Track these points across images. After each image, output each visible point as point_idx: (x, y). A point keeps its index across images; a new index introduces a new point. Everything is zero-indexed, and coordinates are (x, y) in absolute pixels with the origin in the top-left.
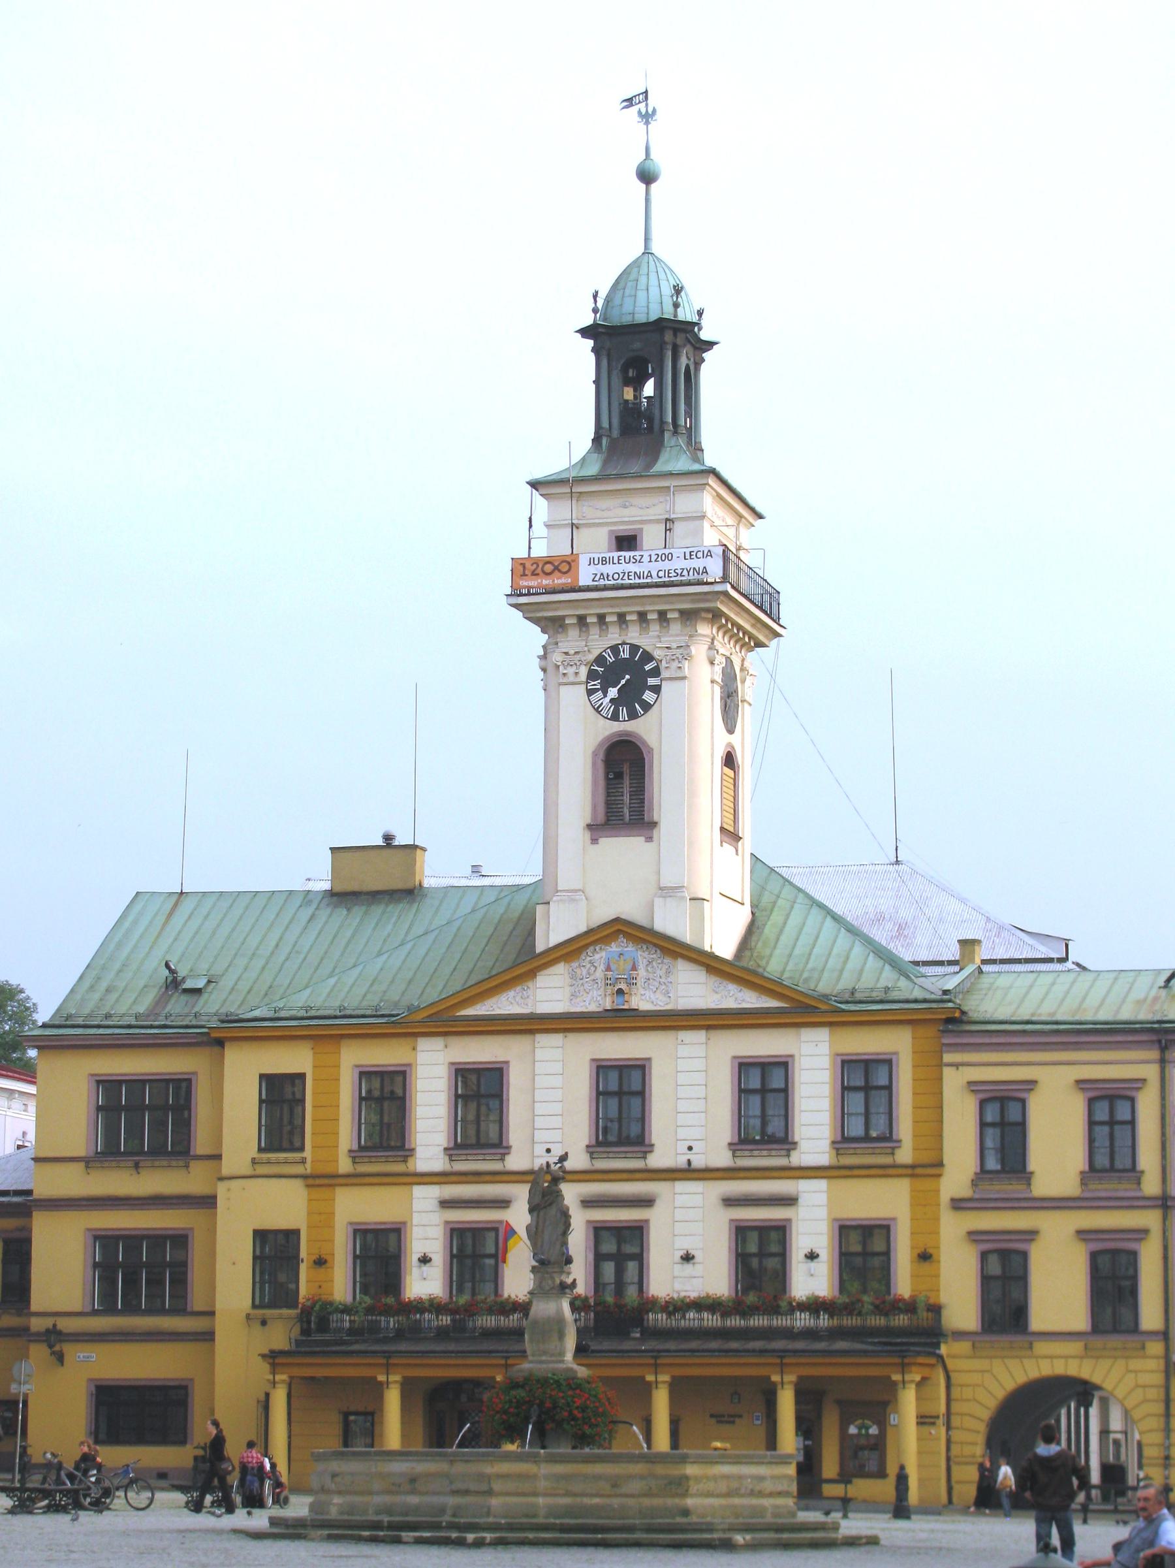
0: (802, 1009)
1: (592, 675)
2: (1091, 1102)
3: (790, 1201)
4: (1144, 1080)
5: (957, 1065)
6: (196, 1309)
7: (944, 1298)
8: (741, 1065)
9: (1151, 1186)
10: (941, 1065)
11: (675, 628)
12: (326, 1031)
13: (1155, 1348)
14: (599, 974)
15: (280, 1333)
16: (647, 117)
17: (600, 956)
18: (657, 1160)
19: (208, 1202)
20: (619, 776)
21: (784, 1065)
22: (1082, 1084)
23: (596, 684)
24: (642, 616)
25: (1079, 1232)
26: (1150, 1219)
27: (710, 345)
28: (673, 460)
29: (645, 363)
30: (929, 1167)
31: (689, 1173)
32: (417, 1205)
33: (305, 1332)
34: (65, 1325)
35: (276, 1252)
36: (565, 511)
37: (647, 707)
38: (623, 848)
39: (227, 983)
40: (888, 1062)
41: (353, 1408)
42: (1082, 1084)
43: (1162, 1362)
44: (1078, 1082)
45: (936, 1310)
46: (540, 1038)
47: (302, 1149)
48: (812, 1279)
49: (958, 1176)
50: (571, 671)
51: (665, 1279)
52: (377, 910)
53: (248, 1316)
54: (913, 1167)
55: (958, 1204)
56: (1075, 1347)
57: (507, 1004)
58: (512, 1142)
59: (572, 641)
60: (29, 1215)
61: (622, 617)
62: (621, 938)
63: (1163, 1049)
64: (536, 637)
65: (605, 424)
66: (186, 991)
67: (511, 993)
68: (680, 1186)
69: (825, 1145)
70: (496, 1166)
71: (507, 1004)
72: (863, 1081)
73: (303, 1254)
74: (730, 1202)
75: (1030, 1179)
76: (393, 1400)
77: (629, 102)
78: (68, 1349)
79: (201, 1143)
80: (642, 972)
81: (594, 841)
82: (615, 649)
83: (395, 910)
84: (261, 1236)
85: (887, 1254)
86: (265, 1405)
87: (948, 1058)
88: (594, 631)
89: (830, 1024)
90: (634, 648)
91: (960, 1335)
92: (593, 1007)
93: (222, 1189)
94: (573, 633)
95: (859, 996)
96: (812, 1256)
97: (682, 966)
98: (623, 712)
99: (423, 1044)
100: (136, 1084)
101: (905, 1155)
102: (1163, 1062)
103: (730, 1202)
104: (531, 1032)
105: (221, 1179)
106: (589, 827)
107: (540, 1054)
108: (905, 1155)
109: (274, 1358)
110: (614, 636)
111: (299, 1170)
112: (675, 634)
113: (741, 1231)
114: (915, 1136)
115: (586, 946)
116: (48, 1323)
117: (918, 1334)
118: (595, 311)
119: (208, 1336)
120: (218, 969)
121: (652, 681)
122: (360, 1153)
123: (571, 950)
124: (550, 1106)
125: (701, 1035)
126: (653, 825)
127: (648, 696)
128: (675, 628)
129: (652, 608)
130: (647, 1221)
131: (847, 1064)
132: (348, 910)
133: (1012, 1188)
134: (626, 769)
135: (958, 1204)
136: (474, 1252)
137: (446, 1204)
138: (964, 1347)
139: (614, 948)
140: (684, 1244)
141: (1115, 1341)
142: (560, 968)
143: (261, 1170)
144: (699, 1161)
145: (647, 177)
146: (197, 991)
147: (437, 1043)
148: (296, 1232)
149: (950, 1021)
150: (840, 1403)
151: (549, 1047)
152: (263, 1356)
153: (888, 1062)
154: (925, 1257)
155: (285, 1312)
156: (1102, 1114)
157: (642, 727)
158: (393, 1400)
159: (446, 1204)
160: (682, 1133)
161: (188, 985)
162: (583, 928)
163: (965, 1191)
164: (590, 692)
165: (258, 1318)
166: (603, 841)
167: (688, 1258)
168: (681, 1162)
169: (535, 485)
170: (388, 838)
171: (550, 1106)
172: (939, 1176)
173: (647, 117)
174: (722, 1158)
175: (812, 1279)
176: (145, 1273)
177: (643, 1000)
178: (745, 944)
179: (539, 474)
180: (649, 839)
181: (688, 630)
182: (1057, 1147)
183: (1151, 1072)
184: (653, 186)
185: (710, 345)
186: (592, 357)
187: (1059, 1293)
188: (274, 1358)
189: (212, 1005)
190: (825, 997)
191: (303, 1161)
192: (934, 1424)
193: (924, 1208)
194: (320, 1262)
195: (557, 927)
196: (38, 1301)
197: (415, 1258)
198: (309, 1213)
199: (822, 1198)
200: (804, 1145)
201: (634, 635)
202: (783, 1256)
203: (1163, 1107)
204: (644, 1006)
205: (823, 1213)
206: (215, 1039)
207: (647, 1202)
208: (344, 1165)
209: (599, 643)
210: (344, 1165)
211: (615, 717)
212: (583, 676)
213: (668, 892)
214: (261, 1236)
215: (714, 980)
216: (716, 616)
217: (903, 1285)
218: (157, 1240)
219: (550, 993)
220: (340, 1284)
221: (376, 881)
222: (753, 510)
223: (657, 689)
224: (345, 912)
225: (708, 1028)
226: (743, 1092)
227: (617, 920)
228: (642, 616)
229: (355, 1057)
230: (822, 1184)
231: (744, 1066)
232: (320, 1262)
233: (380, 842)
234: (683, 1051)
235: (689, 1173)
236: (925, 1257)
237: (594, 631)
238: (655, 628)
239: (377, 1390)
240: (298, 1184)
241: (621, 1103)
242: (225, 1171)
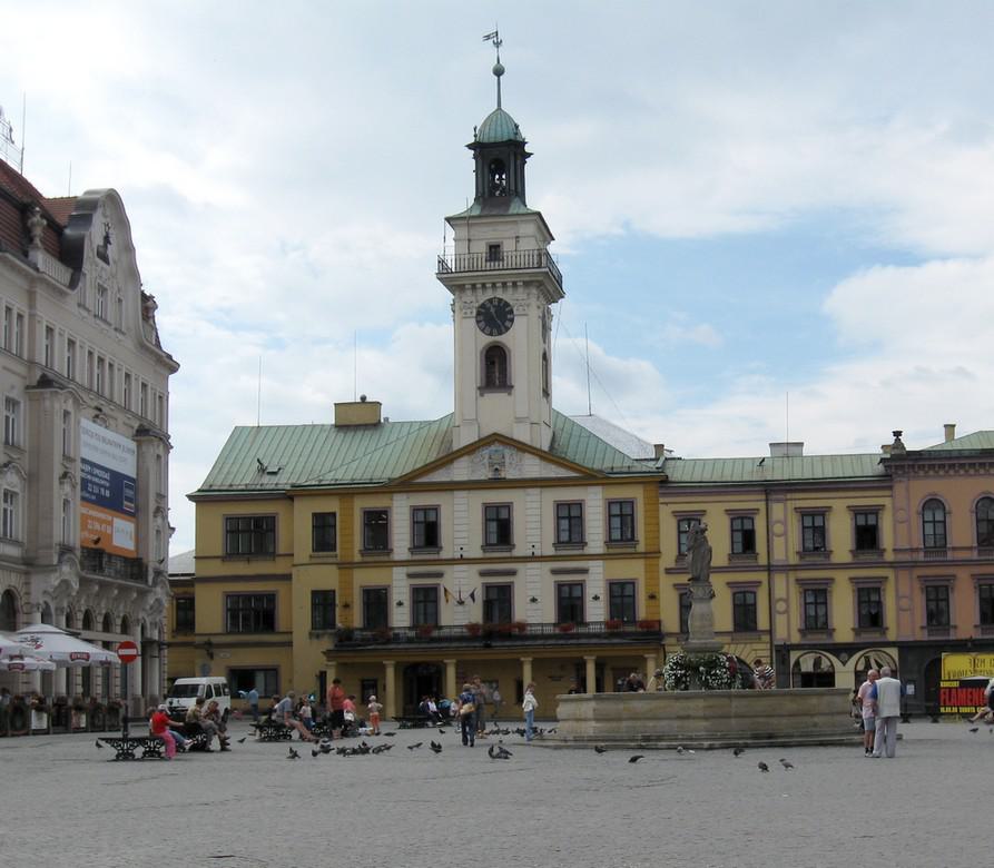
0: (590, 477)
1: (478, 314)
2: (732, 520)
3: (585, 571)
4: (758, 510)
5: (667, 504)
6: (282, 630)
7: (663, 617)
8: (558, 505)
9: (763, 560)
10: (657, 503)
11: (521, 290)
12: (346, 492)
13: (766, 638)
14: (486, 461)
15: (327, 643)
16: (497, 44)
17: (486, 452)
18: (517, 552)
19: (287, 577)
20: (493, 363)
21: (580, 505)
22: (727, 511)
23: (481, 318)
24: (504, 284)
25: (728, 584)
26: (763, 577)
27: (529, 155)
28: (515, 208)
29: (500, 161)
30: (653, 554)
31: (533, 558)
32: (395, 577)
33: (341, 641)
34: (215, 640)
35: (323, 602)
36: (464, 233)
37: (507, 329)
38: (495, 399)
39: (289, 469)
40: (631, 503)
41: (366, 678)
42: (727, 511)
43: (769, 645)
44: (727, 510)
45: (659, 622)
46: (455, 492)
47: (335, 550)
48: (596, 612)
49: (669, 556)
50: (469, 311)
51: (523, 612)
52: (359, 434)
53: (311, 634)
54: (645, 553)
55: (668, 571)
56: (727, 639)
57: (439, 476)
58: (443, 544)
59: (468, 296)
60: (193, 586)
61: (494, 285)
62: (496, 443)
63: (767, 494)
64: (450, 296)
65: (480, 190)
66: (269, 473)
67: (441, 471)
68: (529, 565)
69: (602, 544)
70: (436, 557)
71: (439, 476)
72: (622, 516)
73: (337, 602)
74: (554, 572)
76: (390, 674)
77: (488, 37)
78: (215, 651)
79: (281, 549)
80: (507, 461)
81: (482, 395)
82: (490, 301)
83: (368, 433)
84: (315, 593)
85: (633, 596)
86: (322, 676)
87: (661, 500)
88: (480, 292)
89: (603, 484)
90: (500, 300)
91: (671, 635)
92: (483, 478)
93: (294, 571)
94: (469, 293)
95: (615, 470)
96: (596, 598)
97: (527, 455)
98: (495, 331)
99: (397, 497)
100: (247, 519)
101: (641, 548)
102: (767, 500)
103: (554, 572)
104: (452, 490)
105: (294, 565)
106: (479, 388)
107: (456, 501)
108: (641, 548)
109: (327, 653)
110: (489, 294)
111: (334, 560)
112: (521, 294)
113: (560, 586)
114: (646, 539)
115: (479, 448)
116: (205, 639)
117: (652, 635)
118: (475, 136)
119: (290, 644)
120: (284, 462)
121: (509, 316)
122: (365, 552)
123: (470, 450)
124: (462, 524)
125: (537, 491)
126: (512, 387)
127: (507, 324)
128: (521, 290)
129: (509, 280)
130: (513, 583)
131: (610, 503)
132: (346, 433)
134: (497, 360)
135: (668, 571)
136: (426, 599)
137: (410, 576)
138: (672, 640)
139: (493, 448)
140: (532, 594)
141: (748, 635)
142: (466, 458)
143: (314, 561)
144: (538, 553)
145: (499, 72)
146: (274, 473)
147: (404, 496)
148: (334, 591)
149: (662, 482)
150: (613, 669)
151: (461, 497)
152: (324, 653)
153: (631, 503)
154: (652, 597)
155: (330, 631)
156: (738, 524)
157: (504, 339)
158: (390, 674)
159: (410, 576)
160: (529, 539)
161: (270, 470)
162: (477, 439)
163: (673, 565)
164: (478, 322)
165: (315, 634)
166: (486, 395)
167: (534, 600)
168: (529, 553)
169: (448, 220)
170: (363, 398)
171: (462, 524)
172: (658, 557)
173: (497, 44)
174: (550, 551)
175: (596, 612)
176: (255, 614)
177: (510, 473)
178: (552, 447)
179: (451, 215)
180: (510, 394)
181: (527, 291)
182: (720, 541)
183: (762, 506)
184: (501, 77)
185: (529, 155)
186: (474, 161)
187: (721, 612)
188: (327, 653)
189: (284, 481)
190: (601, 471)
191: (336, 556)
193: (652, 574)
194: (346, 606)
195: (465, 438)
196: (198, 629)
197: (395, 603)
198: (340, 582)
199: (601, 570)
200: (591, 544)
201: (499, 294)
202: (581, 598)
203: (768, 522)
204: (509, 477)
205: (601, 577)
206: (290, 496)
207: (513, 573)
208: (358, 558)
209: (483, 297)
210: (358, 558)
211: (491, 334)
212: (474, 314)
213: (519, 420)
214: (315, 593)
215: (543, 463)
216: (540, 284)
217: (642, 613)
218: (259, 597)
219: (461, 471)
220: (357, 619)
221: (359, 419)
222: (551, 235)
223: (512, 320)
224: (343, 435)
225: (542, 487)
226: (559, 518)
227: (495, 434)
228: (504, 284)
229: (362, 504)
230: (600, 563)
231: (559, 505)
232: (346, 606)
233: (359, 400)
234: (529, 499)
235: (533, 558)
236: (652, 597)
237: (480, 292)
238: (510, 290)
239: (382, 668)
240: (334, 567)
241: (500, 528)
242: (296, 562)
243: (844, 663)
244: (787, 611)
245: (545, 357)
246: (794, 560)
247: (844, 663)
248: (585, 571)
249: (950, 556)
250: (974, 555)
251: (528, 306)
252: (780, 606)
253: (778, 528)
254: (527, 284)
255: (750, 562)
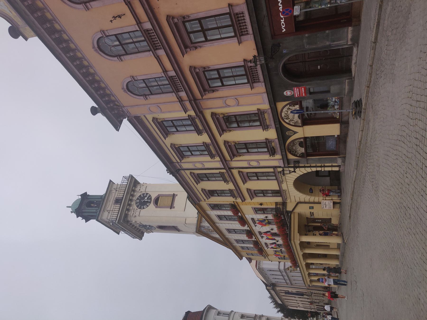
5: (205, 200)
26: (235, 172)
45: (276, 204)
55: (243, 199)
75: (231, 190)
89: (204, 211)
128: (131, 222)
133: (235, 192)
135: (243, 199)
192: (313, 213)
216: (126, 215)
219: (217, 236)
243: (295, 133)
244: (258, 161)
245: (156, 201)
246: (218, 159)
247: (295, 133)
248: (253, 219)
249: (172, 73)
250: (161, 53)
251: (136, 222)
252: (254, 164)
253: (199, 166)
254: (128, 222)
255: (226, 175)
